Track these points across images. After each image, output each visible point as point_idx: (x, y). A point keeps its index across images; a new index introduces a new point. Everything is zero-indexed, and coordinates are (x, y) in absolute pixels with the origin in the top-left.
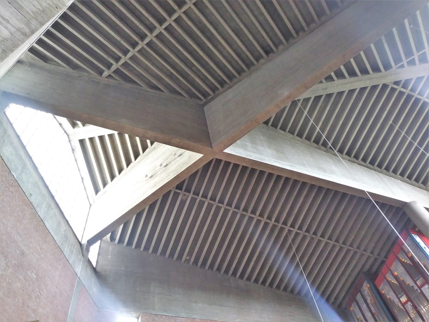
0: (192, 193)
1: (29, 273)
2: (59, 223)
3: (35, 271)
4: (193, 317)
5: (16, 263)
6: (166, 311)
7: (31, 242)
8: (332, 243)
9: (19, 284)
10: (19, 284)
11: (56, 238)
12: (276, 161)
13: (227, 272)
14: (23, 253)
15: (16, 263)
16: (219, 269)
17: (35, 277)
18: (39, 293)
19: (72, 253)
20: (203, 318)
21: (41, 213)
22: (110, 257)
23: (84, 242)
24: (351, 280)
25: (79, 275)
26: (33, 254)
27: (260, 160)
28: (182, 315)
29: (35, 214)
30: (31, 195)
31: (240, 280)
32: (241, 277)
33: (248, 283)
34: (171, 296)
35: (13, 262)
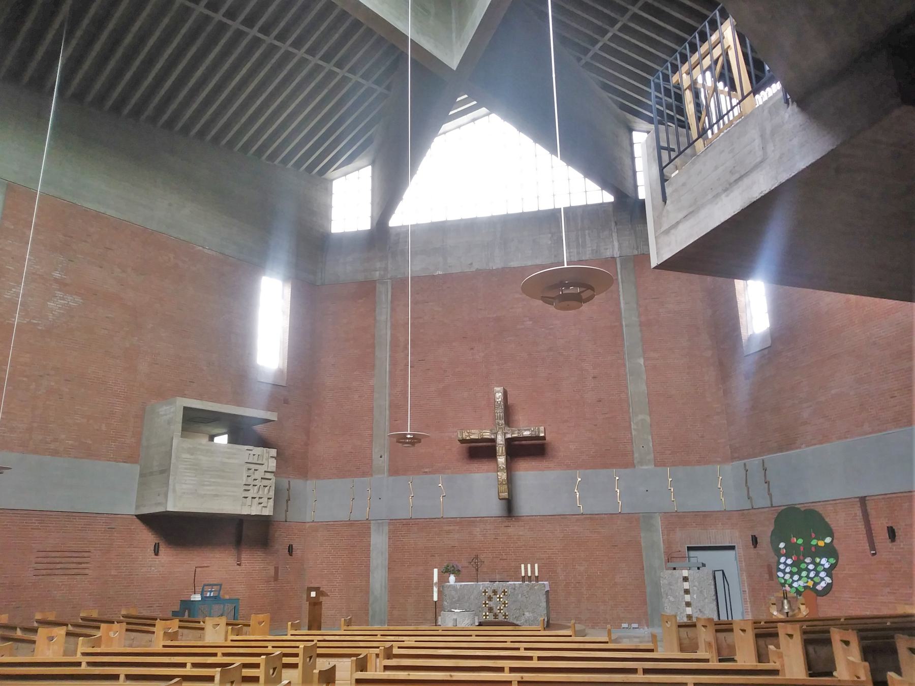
0: (629, 7)
25: (616, 254)
30: (471, 264)
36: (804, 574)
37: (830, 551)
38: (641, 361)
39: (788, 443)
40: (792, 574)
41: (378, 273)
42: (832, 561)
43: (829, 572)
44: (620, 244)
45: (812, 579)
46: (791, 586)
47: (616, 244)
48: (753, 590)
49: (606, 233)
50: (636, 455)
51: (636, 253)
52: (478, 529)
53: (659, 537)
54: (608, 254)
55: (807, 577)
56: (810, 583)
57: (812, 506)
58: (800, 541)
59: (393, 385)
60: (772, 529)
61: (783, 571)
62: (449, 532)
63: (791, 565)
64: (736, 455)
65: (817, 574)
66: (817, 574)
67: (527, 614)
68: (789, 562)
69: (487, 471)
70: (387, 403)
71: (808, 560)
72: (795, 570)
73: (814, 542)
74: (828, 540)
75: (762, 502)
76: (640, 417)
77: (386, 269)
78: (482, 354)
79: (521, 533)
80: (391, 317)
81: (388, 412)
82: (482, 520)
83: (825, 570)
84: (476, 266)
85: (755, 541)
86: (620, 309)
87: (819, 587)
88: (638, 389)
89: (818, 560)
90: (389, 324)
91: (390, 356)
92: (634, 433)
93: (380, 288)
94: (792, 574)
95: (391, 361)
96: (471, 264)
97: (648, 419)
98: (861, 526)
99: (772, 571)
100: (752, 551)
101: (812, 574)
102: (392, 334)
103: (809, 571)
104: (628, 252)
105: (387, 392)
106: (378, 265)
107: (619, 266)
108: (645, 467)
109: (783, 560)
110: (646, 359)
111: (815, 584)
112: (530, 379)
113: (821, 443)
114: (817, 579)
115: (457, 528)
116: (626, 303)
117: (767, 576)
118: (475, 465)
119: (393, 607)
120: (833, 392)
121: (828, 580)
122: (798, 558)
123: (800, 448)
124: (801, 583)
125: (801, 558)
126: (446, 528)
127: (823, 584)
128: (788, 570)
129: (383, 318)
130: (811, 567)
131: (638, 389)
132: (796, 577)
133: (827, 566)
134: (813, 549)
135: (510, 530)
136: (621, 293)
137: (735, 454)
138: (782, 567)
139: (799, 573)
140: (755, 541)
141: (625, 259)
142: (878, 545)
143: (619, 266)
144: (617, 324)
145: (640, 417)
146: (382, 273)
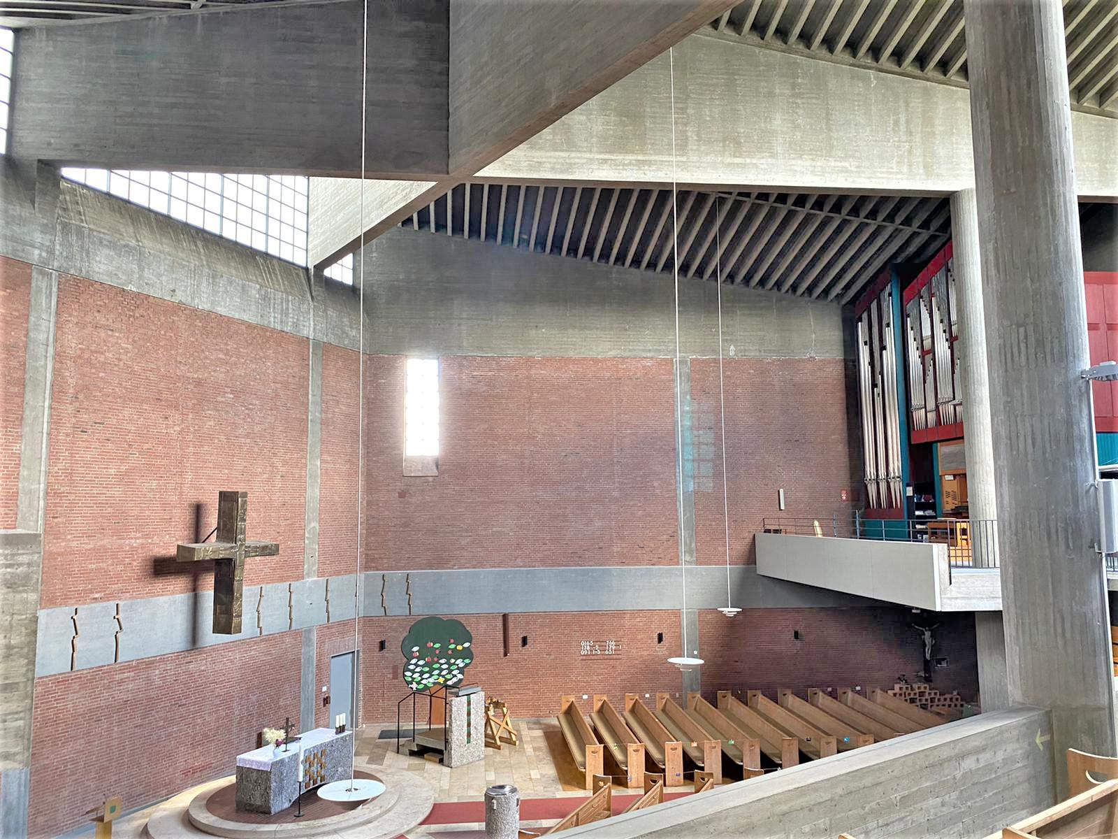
1: (220, 399)
2: (243, 288)
3: (229, 390)
4: (530, 354)
5: (195, 402)
6: (480, 348)
7: (206, 358)
8: (821, 215)
9: (212, 423)
10: (212, 423)
11: (245, 317)
12: (605, 161)
13: (605, 255)
14: (199, 383)
15: (195, 402)
16: (589, 251)
17: (232, 396)
18: (246, 412)
19: (287, 314)
20: (547, 354)
21: (203, 304)
22: (375, 255)
23: (311, 267)
24: (871, 271)
26: (215, 371)
27: (562, 172)
28: (510, 352)
29: (194, 313)
30: (174, 291)
31: (633, 270)
32: (636, 262)
33: (650, 273)
34: (491, 320)
35: (190, 404)
36: (436, 672)
37: (467, 654)
38: (318, 463)
39: (439, 562)
40: (422, 673)
41: (37, 252)
42: (467, 661)
43: (461, 670)
44: (315, 325)
45: (443, 676)
46: (418, 683)
47: (312, 323)
48: (369, 691)
49: (305, 306)
50: (306, 567)
51: (325, 340)
52: (157, 672)
53: (314, 652)
54: (305, 333)
55: (439, 675)
56: (441, 680)
57: (454, 618)
58: (437, 645)
59: (53, 456)
60: (405, 634)
61: (413, 672)
62: (121, 682)
63: (423, 666)
64: (374, 565)
65: (449, 673)
66: (450, 672)
67: (340, 769)
68: (421, 662)
69: (173, 593)
70: (42, 486)
71: (442, 661)
72: (427, 669)
73: (452, 646)
74: (467, 645)
75: (397, 608)
76: (313, 525)
77: (51, 252)
78: (177, 428)
79: (203, 668)
80: (56, 340)
81: (42, 503)
82: (163, 659)
83: (458, 668)
84: (180, 296)
85: (382, 645)
86: (308, 399)
87: (450, 683)
88: (314, 493)
89: (453, 661)
90: (51, 350)
91: (51, 408)
92: (306, 542)
93: (38, 281)
94: (422, 673)
95: (51, 415)
96: (174, 291)
97: (317, 526)
98: (500, 635)
99: (398, 672)
100: (377, 654)
101: (444, 673)
102: (54, 369)
103: (442, 670)
104: (320, 336)
105: (43, 468)
106: (38, 237)
107: (311, 350)
108: (310, 579)
109: (414, 661)
110: (323, 461)
111: (447, 680)
112: (226, 471)
113: (474, 568)
114: (448, 677)
115: (132, 674)
116: (313, 395)
117: (390, 676)
118: (160, 584)
119: (38, 813)
120: (494, 529)
121: (460, 676)
122: (433, 659)
123: (452, 568)
124: (431, 680)
125: (436, 659)
126: (118, 677)
127: (455, 680)
128: (418, 669)
129: (42, 337)
130: (445, 666)
131: (314, 493)
132: (426, 676)
133: (461, 665)
134: (450, 652)
135: (191, 666)
136: (310, 383)
137: (370, 563)
138: (411, 667)
139: (432, 670)
140: (382, 645)
141: (317, 344)
142: (511, 649)
143: (311, 350)
144: (304, 417)
145: (313, 525)
146: (44, 254)
